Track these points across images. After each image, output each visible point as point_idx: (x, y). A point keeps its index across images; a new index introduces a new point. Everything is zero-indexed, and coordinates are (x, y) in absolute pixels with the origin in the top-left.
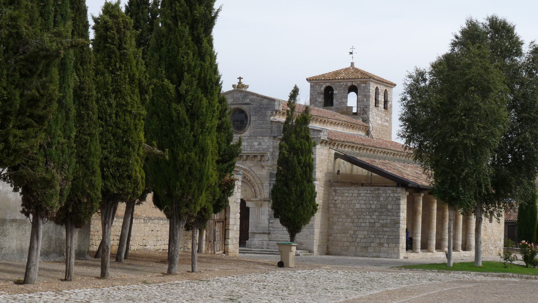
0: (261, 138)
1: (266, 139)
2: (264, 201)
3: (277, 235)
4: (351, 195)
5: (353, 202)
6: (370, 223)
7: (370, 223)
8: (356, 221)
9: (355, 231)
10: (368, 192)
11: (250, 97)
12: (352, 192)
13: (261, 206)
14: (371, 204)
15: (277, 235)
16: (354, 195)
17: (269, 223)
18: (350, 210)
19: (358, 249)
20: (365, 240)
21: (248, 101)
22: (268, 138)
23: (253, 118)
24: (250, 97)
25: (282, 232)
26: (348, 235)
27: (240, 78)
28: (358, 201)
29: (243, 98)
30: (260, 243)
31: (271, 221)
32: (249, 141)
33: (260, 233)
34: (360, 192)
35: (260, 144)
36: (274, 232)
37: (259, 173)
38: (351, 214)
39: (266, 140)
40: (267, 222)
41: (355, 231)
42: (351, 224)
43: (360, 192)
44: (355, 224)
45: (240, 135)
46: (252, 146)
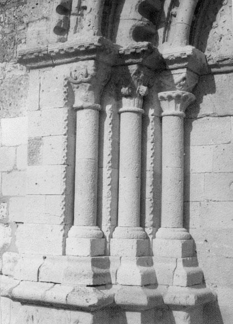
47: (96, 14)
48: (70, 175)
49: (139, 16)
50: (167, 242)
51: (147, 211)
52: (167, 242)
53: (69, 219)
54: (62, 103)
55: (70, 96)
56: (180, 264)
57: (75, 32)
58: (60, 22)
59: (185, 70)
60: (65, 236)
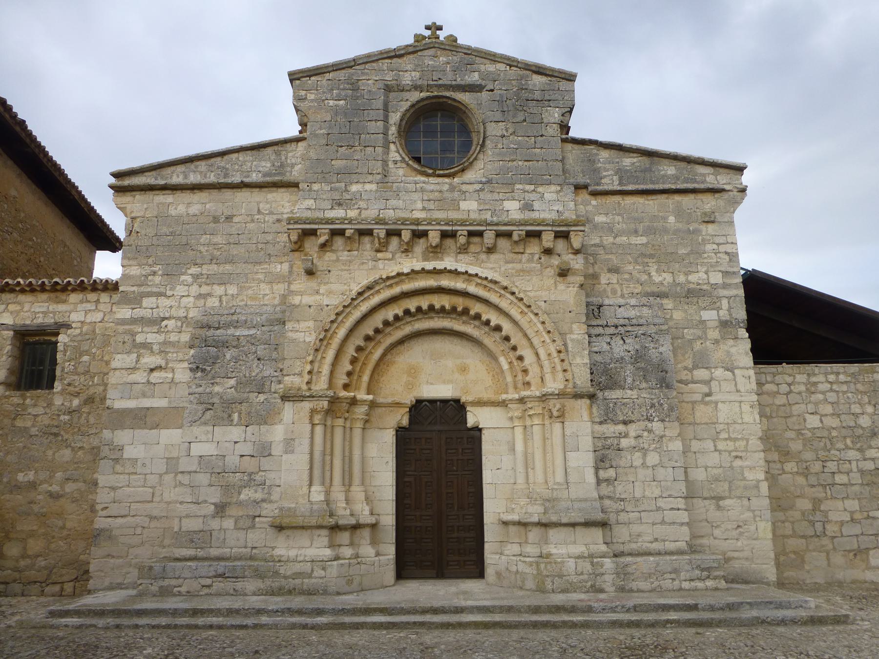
0: (532, 187)
1: (550, 193)
2: (577, 396)
3: (636, 528)
4: (784, 388)
5: (796, 409)
6: (862, 472)
7: (862, 472)
8: (817, 467)
9: (817, 503)
10: (842, 378)
12: (789, 379)
13: (561, 416)
14: (856, 415)
15: (636, 528)
16: (796, 388)
18: (791, 434)
19: (838, 559)
20: (857, 530)
21: (475, 78)
22: (553, 188)
23: (494, 130)
25: (658, 517)
26: (797, 515)
28: (811, 408)
31: (602, 474)
33: (573, 525)
34: (814, 379)
36: (623, 517)
37: (544, 295)
38: (796, 446)
40: (591, 478)
41: (817, 503)
42: (801, 480)
43: (814, 379)
44: (813, 480)
45: (447, 180)
54: (307, 421)
55: (311, 418)
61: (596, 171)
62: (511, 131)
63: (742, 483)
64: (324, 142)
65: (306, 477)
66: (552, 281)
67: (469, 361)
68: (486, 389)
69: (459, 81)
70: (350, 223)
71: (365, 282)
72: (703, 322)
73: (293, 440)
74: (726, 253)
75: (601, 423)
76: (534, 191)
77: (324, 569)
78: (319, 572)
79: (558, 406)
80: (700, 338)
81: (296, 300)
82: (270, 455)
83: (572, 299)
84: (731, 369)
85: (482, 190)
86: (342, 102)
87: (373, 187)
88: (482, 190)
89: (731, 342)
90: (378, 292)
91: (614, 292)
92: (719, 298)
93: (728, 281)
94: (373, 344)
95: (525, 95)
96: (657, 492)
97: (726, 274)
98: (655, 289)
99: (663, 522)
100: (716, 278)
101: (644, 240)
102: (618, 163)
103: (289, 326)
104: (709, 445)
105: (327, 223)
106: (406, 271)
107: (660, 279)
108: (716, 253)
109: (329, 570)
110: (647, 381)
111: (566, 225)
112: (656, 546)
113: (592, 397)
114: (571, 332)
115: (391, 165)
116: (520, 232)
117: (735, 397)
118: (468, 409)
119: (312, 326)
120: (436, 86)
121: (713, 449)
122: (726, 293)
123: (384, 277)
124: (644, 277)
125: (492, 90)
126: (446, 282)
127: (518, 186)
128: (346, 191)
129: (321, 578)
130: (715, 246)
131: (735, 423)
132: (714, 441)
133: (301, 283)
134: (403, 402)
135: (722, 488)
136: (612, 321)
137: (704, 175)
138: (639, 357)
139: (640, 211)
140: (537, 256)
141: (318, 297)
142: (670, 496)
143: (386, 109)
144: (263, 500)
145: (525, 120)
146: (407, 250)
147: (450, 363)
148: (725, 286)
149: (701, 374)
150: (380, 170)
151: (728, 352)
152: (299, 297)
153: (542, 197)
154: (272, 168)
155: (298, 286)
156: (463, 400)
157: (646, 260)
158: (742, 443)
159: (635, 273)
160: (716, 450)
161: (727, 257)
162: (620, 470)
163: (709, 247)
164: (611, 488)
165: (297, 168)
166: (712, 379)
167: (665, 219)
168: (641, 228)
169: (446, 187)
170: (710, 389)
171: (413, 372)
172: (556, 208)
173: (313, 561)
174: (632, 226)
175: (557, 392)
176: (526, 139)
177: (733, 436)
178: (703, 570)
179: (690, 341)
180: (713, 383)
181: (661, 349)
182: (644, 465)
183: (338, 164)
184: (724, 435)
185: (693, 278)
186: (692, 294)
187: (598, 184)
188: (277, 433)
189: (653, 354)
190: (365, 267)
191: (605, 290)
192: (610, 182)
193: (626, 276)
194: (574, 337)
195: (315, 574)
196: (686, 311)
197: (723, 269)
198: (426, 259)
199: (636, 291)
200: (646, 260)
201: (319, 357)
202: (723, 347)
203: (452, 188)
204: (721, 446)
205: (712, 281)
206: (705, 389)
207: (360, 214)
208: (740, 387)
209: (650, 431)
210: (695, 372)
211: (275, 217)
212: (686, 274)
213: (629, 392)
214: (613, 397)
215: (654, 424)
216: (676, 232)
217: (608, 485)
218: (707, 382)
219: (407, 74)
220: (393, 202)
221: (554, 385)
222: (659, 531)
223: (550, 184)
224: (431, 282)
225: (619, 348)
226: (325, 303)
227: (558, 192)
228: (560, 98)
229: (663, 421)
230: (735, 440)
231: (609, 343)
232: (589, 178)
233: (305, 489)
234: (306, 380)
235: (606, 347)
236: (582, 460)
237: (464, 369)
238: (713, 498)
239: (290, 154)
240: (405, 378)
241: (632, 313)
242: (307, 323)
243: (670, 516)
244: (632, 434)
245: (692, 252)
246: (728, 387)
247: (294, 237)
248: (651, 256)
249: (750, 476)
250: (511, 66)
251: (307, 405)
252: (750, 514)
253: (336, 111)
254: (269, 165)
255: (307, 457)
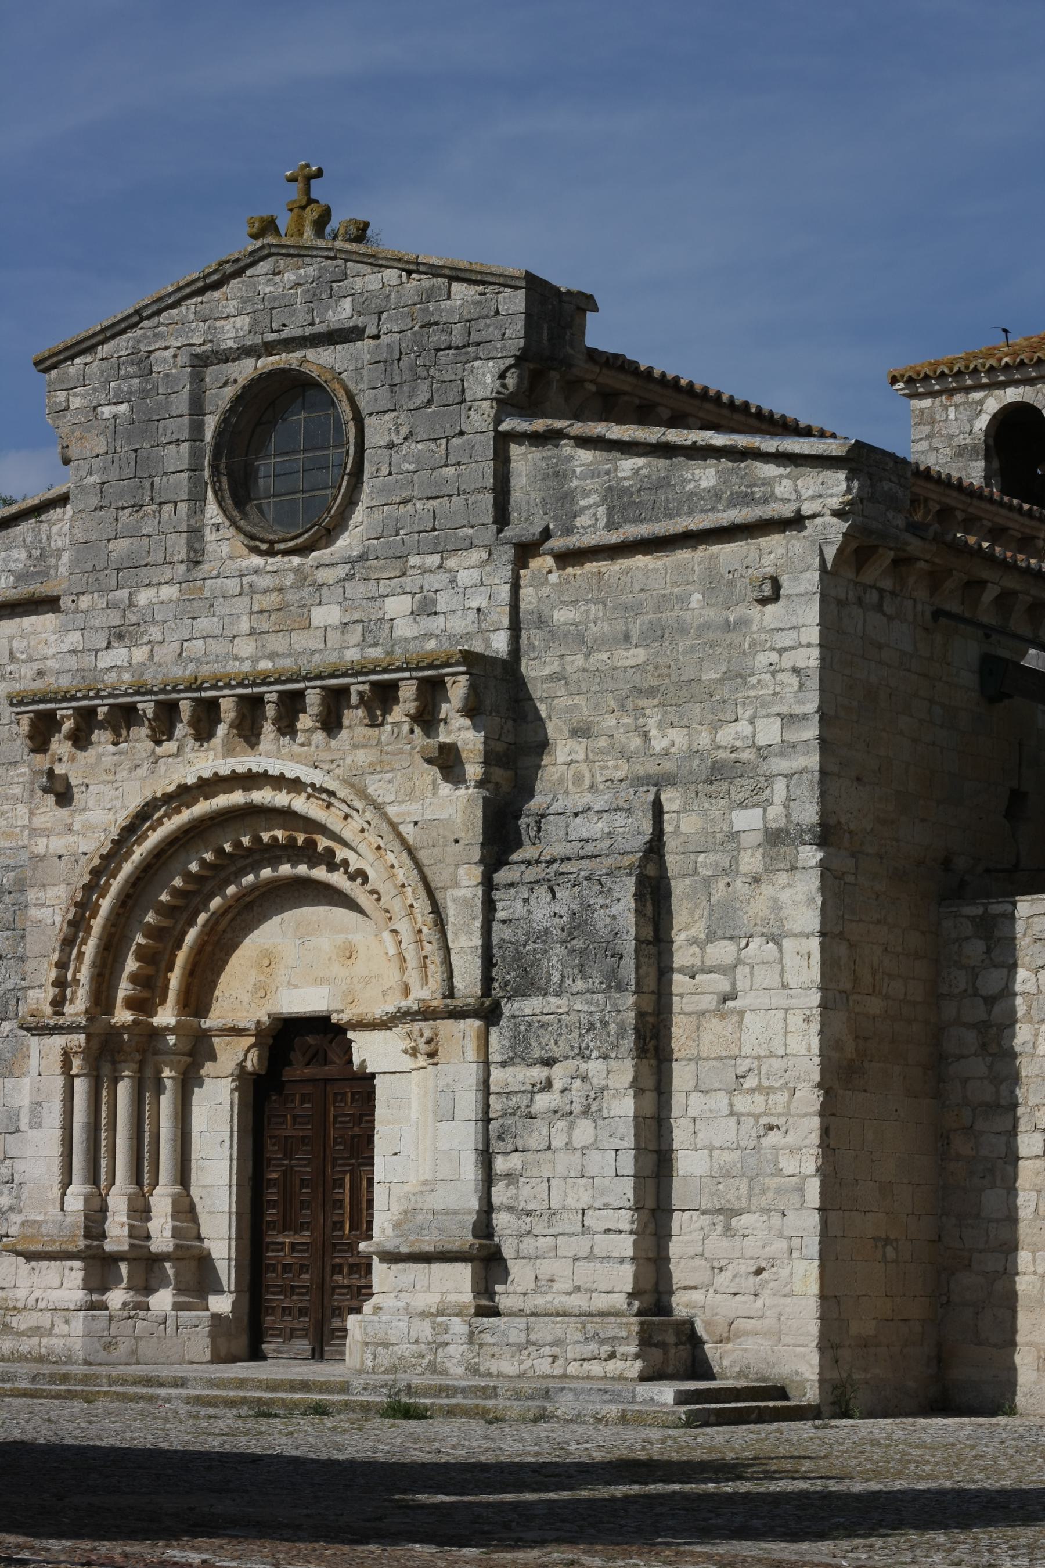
1: (467, 567)
3: (547, 1267)
11: (358, 284)
15: (547, 1267)
17: (488, 1178)
21: (342, 313)
22: (477, 555)
23: (377, 431)
24: (358, 284)
25: (582, 1245)
27: (309, 177)
29: (313, 298)
30: (424, 1329)
32: (357, 590)
35: (426, 608)
36: (528, 1245)
39: (465, 577)
45: (296, 560)
46: (373, 628)
47: (87, 988)
48: (67, 1137)
49: (131, 986)
50: (161, 1202)
51: (141, 1175)
52: (161, 1202)
53: (66, 1182)
54: (59, 1071)
56: (169, 1219)
57: (70, 1003)
58: (55, 996)
59: (174, 1037)
60: (64, 1194)
61: (567, 498)
62: (404, 431)
63: (773, 1182)
64: (94, 501)
65: (56, 1168)
66: (429, 780)
67: (356, 938)
68: (384, 994)
69: (319, 328)
70: (97, 696)
71: (135, 802)
72: (734, 836)
73: (39, 1104)
74: (795, 670)
75: (504, 1064)
76: (440, 567)
77: (67, 1322)
78: (61, 1328)
79: (427, 1034)
80: (725, 872)
81: (40, 846)
82: (18, 1130)
83: (460, 814)
84: (774, 939)
85: (350, 577)
86: (124, 408)
87: (169, 592)
88: (350, 577)
89: (783, 878)
90: (160, 822)
91: (578, 779)
92: (770, 778)
93: (791, 737)
94: (185, 916)
95: (437, 338)
96: (585, 1200)
97: (789, 720)
98: (651, 768)
99: (590, 1257)
100: (769, 732)
101: (638, 655)
102: (608, 473)
103: (32, 895)
104: (720, 1102)
105: (64, 699)
106: (190, 780)
107: (665, 743)
108: (774, 674)
109: (73, 1324)
110: (584, 978)
111: (431, 666)
112: (577, 1302)
113: (489, 1014)
114: (456, 884)
115: (210, 536)
116: (361, 687)
117: (779, 999)
118: (350, 1035)
119: (63, 896)
120: (279, 342)
121: (726, 1111)
122: (782, 765)
123: (159, 795)
124: (636, 742)
125: (376, 337)
126: (262, 796)
127: (414, 560)
128: (131, 605)
129: (63, 1336)
130: (774, 657)
131: (771, 1055)
132: (731, 1093)
133: (48, 811)
134: (242, 1025)
135: (734, 1192)
136: (559, 849)
137: (767, 482)
138: (577, 925)
139: (637, 587)
140: (406, 728)
141: (71, 839)
142: (606, 1207)
143: (197, 408)
144: (11, 1209)
145: (430, 401)
146: (203, 733)
147: (325, 943)
148: (788, 748)
149: (722, 951)
150: (183, 555)
151: (775, 900)
152: (44, 840)
153: (453, 581)
154: (29, 562)
155: (43, 818)
156: (335, 1018)
157: (641, 703)
158: (780, 1099)
159: (620, 737)
160: (732, 1114)
161: (794, 681)
162: (530, 1156)
163: (764, 659)
164: (512, 1191)
165: (65, 557)
166: (739, 962)
167: (683, 600)
168: (635, 629)
169: (289, 579)
170: (734, 984)
171: (268, 960)
172: (475, 605)
173: (56, 1310)
174: (620, 626)
175: (415, 1008)
176: (432, 445)
177: (765, 1083)
178: (603, 1342)
179: (707, 881)
180: (741, 971)
181: (615, 909)
182: (569, 1147)
183: (120, 546)
184: (750, 1082)
185: (726, 736)
186: (720, 773)
187: (569, 531)
188: (22, 1092)
189: (601, 920)
190: (140, 772)
191: (562, 780)
192: (591, 528)
193: (603, 742)
194: (461, 892)
195: (56, 1331)
196: (705, 813)
197: (785, 710)
198: (229, 751)
199: (619, 774)
200: (641, 703)
201: (75, 952)
202: (767, 890)
203: (302, 577)
204: (742, 1103)
205: (761, 741)
206: (723, 984)
207: (151, 656)
208: (791, 980)
209: (584, 1079)
210: (710, 949)
211: (36, 666)
212: (716, 726)
213: (552, 999)
214: (528, 1011)
215: (591, 1063)
216: (705, 627)
217: (507, 1185)
218: (728, 970)
219: (227, 325)
220: (204, 624)
221: (426, 992)
222: (585, 1272)
223: (471, 546)
224: (237, 798)
225: (544, 911)
226: (80, 851)
227: (482, 564)
228: (494, 333)
229: (606, 1057)
230: (768, 1091)
231: (526, 901)
232: (555, 518)
233: (56, 1192)
234: (50, 998)
235: (519, 909)
236: (464, 1136)
237: (350, 954)
238: (719, 1211)
239: (55, 529)
240: (253, 976)
241: (597, 827)
242: (56, 889)
243: (603, 1244)
244: (558, 1085)
245: (726, 677)
246: (766, 977)
247: (25, 728)
248: (651, 692)
249: (788, 1164)
250: (410, 273)
251: (58, 1041)
252: (783, 1245)
253: (114, 428)
254: (23, 555)
255: (57, 1134)
